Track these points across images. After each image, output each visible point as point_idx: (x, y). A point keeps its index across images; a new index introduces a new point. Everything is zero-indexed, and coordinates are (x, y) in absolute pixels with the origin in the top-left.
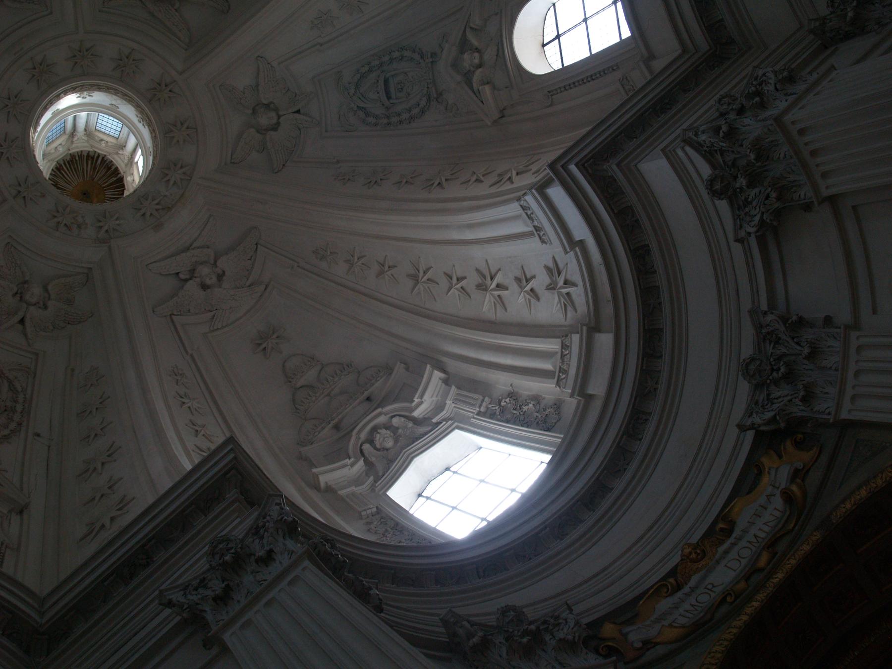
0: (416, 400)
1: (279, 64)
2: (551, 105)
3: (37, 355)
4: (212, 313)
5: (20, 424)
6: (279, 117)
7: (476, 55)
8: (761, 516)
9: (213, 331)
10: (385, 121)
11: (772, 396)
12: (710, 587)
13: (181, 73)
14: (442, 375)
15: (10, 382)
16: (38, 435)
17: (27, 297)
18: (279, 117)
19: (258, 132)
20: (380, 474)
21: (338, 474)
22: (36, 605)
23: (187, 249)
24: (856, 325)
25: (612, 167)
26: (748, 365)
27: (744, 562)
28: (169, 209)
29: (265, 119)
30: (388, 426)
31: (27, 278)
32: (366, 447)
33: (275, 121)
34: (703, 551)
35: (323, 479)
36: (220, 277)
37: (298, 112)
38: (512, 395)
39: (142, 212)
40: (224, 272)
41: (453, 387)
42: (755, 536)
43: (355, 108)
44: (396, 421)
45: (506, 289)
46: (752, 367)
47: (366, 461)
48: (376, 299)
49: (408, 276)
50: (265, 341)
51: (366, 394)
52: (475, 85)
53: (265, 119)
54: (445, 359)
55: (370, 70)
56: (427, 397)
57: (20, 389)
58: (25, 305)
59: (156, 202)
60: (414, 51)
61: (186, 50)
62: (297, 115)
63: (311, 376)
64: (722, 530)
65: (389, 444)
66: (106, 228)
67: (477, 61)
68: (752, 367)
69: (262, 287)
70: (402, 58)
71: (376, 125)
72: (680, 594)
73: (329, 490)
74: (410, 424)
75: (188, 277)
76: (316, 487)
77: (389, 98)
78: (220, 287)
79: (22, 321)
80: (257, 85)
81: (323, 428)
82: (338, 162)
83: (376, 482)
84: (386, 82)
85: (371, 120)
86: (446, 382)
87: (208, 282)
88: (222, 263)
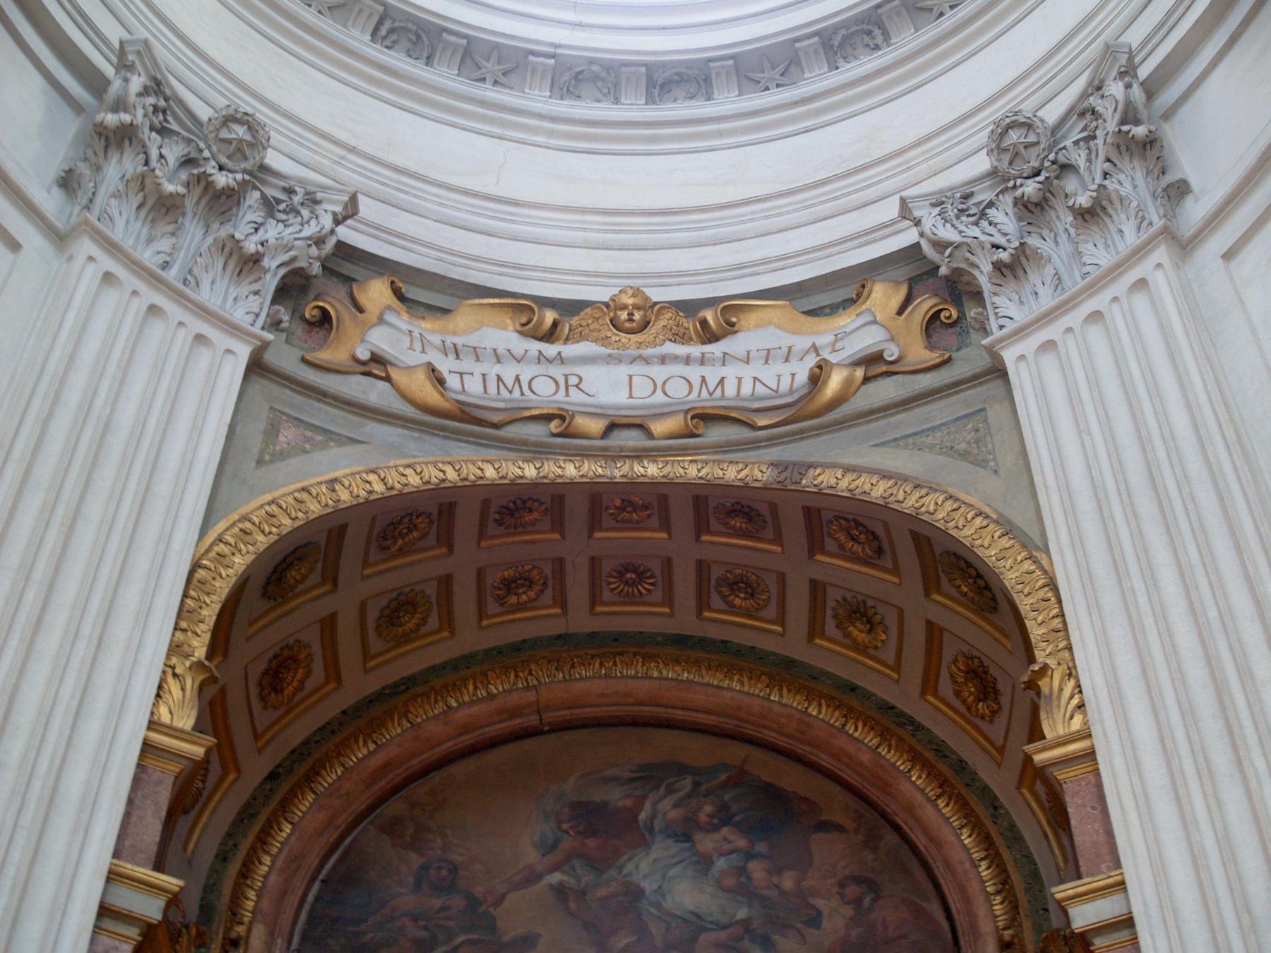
11: (991, 212)
12: (573, 380)
24: (1185, 246)
26: (1013, 125)
27: (659, 398)
34: (645, 325)
42: (722, 381)
46: (1014, 136)
64: (704, 323)
72: (535, 346)
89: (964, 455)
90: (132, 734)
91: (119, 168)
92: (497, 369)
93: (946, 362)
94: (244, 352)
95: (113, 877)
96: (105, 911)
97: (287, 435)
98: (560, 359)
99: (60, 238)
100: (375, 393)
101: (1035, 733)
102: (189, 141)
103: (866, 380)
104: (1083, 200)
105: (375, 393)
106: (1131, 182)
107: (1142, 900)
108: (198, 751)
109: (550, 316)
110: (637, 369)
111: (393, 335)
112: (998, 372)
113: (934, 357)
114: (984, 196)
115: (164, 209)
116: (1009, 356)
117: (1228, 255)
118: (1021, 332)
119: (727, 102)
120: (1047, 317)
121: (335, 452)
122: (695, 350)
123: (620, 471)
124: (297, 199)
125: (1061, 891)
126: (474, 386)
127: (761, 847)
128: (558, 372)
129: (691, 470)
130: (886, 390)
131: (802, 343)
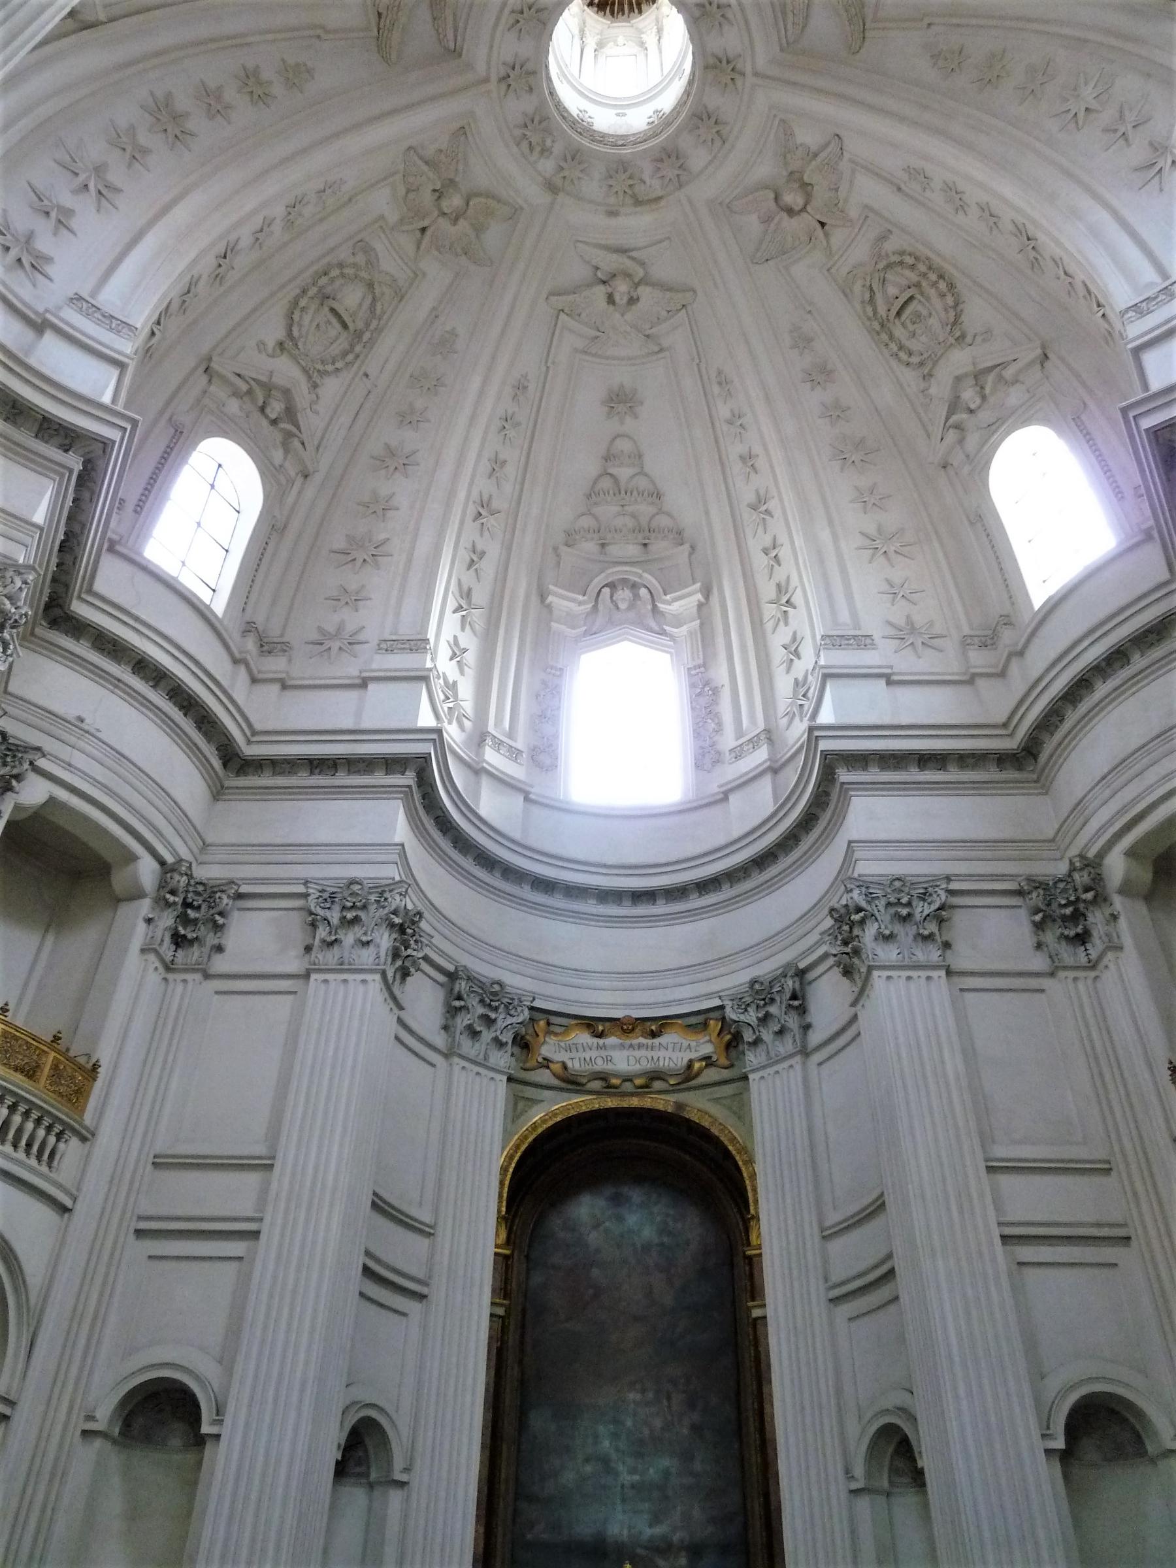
0: (668, 597)
1: (851, 161)
2: (972, 524)
3: (416, 275)
4: (598, 334)
5: (357, 356)
6: (804, 209)
7: (978, 401)
8: (674, 1052)
9: (586, 353)
10: (877, 327)
13: (756, 74)
14: (703, 600)
15: (374, 299)
16: (367, 375)
17: (445, 205)
18: (804, 209)
19: (776, 199)
20: (594, 629)
21: (566, 603)
22: (249, 734)
23: (622, 251)
25: (844, 775)
27: (638, 1067)
28: (638, 202)
29: (793, 198)
30: (634, 586)
31: (457, 179)
32: (607, 590)
33: (797, 208)
34: (633, 1029)
35: (550, 599)
36: (632, 301)
37: (823, 224)
38: (716, 691)
39: (611, 182)
40: (638, 299)
41: (698, 621)
43: (868, 284)
44: (643, 592)
45: (786, 624)
47: (595, 607)
48: (724, 473)
49: (757, 491)
50: (621, 401)
51: (647, 541)
52: (951, 421)
53: (793, 198)
54: (715, 591)
55: (912, 267)
56: (676, 605)
57: (378, 312)
58: (436, 213)
59: (631, 182)
60: (956, 304)
61: (782, 50)
62: (818, 226)
63: (624, 473)
65: (623, 606)
66: (566, 173)
67: (973, 406)
68: (757, 986)
69: (656, 349)
70: (943, 296)
71: (869, 319)
72: (596, 1040)
73: (549, 607)
74: (650, 607)
75: (604, 278)
76: (542, 597)
77: (899, 314)
78: (623, 315)
79: (423, 230)
80: (816, 155)
81: (592, 539)
82: (810, 312)
83: (585, 634)
84: (911, 298)
85: (869, 310)
86: (700, 606)
87: (617, 298)
88: (644, 292)
89: (735, 1113)
90: (491, 1250)
91: (462, 1021)
92: (583, 1055)
93: (732, 1066)
94: (505, 1078)
95: (492, 1304)
96: (492, 1315)
97: (521, 1105)
98: (604, 1047)
99: (446, 1056)
100: (544, 1076)
101: (749, 1244)
102: (481, 995)
103: (707, 1065)
104: (777, 1028)
105: (544, 1076)
106: (792, 1021)
107: (770, 1312)
108: (507, 1252)
109: (601, 1028)
110: (631, 1052)
111: (550, 1048)
112: (745, 1078)
113: (726, 1063)
114: (748, 1000)
115: (474, 1034)
116: (751, 1077)
117: (820, 1064)
118: (753, 1071)
119: (661, 908)
120: (764, 1067)
121: (536, 1108)
122: (650, 1042)
123: (626, 1103)
124: (516, 1002)
125: (750, 1304)
126: (577, 1065)
127: (672, 1212)
128: (604, 1053)
129: (647, 1102)
130: (711, 1075)
131: (685, 1043)
